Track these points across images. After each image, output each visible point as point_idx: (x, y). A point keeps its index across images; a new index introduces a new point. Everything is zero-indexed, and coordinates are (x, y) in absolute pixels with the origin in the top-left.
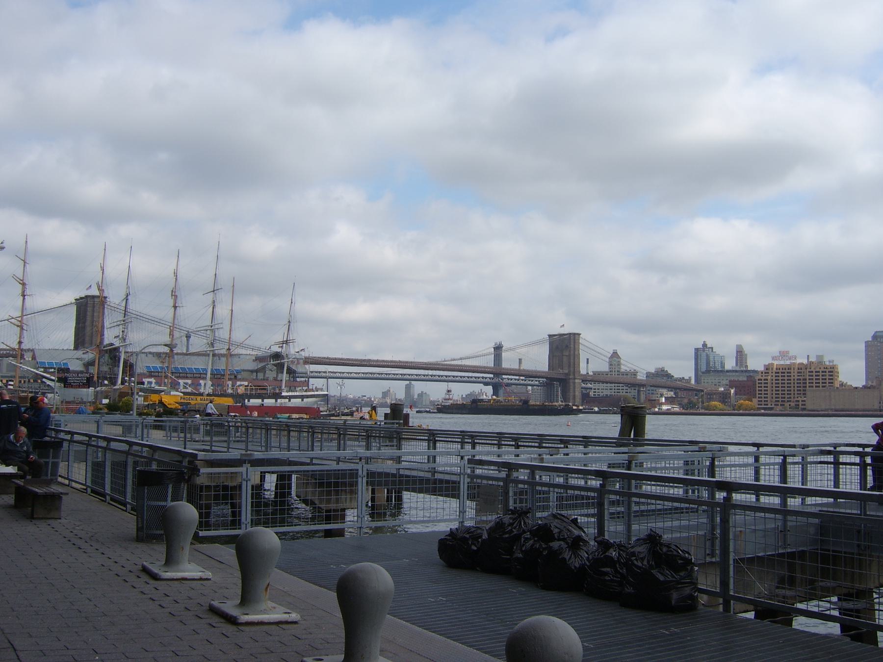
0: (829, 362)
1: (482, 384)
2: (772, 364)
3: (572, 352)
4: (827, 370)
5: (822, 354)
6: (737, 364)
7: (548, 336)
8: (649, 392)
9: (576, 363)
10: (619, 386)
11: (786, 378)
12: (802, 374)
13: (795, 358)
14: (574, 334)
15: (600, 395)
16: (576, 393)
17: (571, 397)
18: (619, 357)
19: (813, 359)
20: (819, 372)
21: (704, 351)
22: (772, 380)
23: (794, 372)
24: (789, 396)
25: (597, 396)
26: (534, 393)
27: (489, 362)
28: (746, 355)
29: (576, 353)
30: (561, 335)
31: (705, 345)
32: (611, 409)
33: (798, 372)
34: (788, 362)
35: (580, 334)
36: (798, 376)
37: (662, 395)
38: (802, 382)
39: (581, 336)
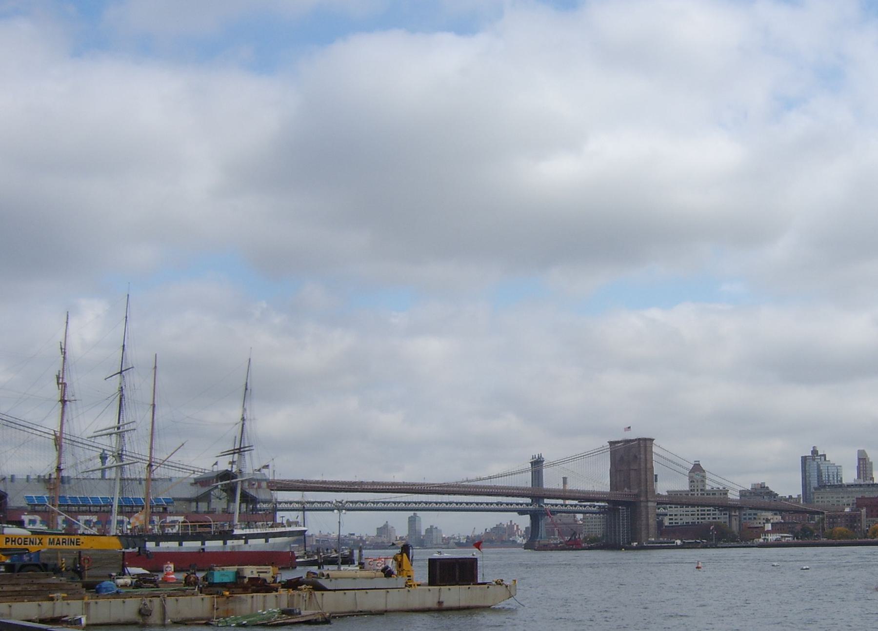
1: (516, 513)
3: (643, 465)
7: (608, 444)
8: (745, 517)
9: (648, 480)
10: (704, 510)
14: (645, 440)
15: (678, 523)
16: (650, 522)
17: (643, 528)
21: (814, 460)
25: (674, 524)
26: (587, 524)
28: (871, 463)
29: (649, 466)
31: (815, 452)
32: (698, 541)
35: (653, 440)
37: (768, 521)
39: (654, 442)
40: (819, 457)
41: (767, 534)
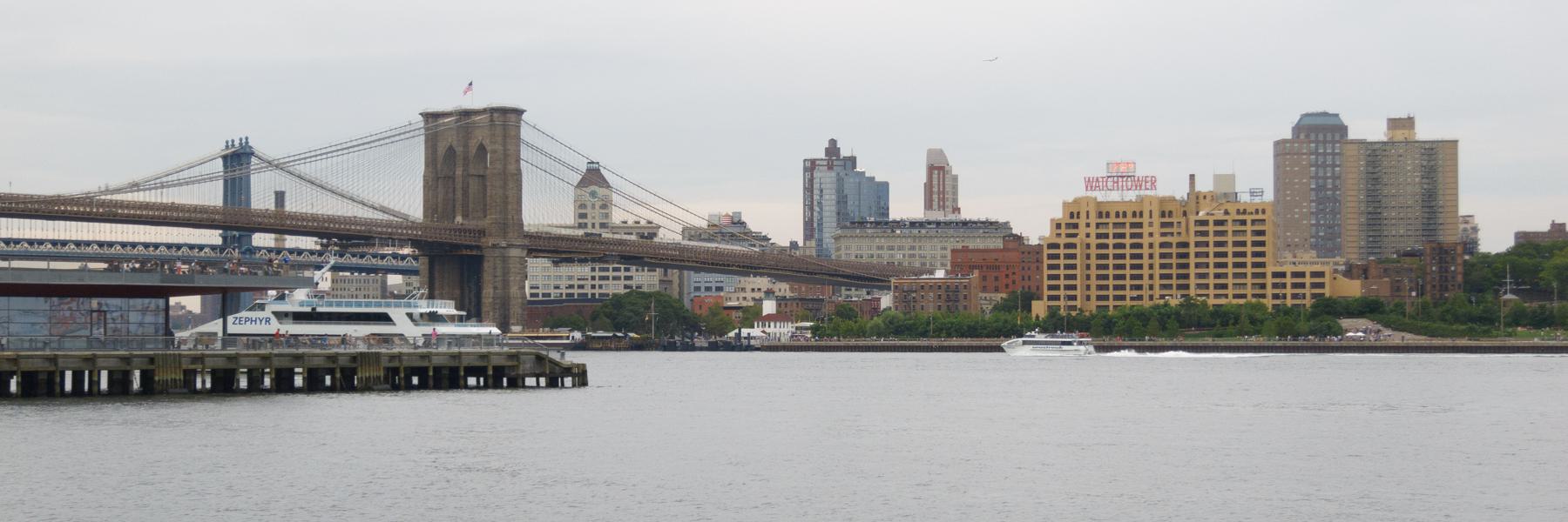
0: (1252, 193)
2: (1087, 200)
4: (1249, 218)
5: (1230, 172)
6: (929, 205)
7: (421, 118)
10: (607, 270)
11: (1128, 241)
12: (1175, 230)
13: (1153, 184)
14: (504, 111)
15: (549, 295)
18: (604, 183)
19: (1205, 185)
22: (1088, 246)
23: (1151, 224)
24: (1135, 293)
25: (540, 298)
27: (212, 196)
28: (955, 178)
31: (832, 149)
32: (619, 334)
33: (1163, 225)
34: (1131, 196)
36: (1163, 234)
38: (1174, 250)
39: (524, 116)
41: (767, 323)
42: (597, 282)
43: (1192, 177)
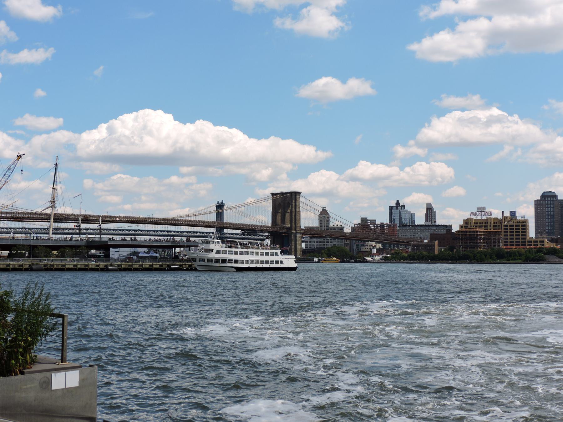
0: (521, 217)
2: (471, 219)
3: (293, 209)
4: (520, 224)
6: (427, 220)
12: (498, 228)
13: (491, 214)
19: (507, 214)
20: (513, 226)
21: (397, 209)
23: (490, 226)
27: (213, 218)
28: (435, 212)
29: (297, 210)
30: (282, 194)
31: (398, 203)
33: (494, 226)
34: (484, 218)
35: (300, 193)
37: (374, 247)
39: (301, 194)
40: (401, 207)
42: (325, 243)
43: (503, 212)
